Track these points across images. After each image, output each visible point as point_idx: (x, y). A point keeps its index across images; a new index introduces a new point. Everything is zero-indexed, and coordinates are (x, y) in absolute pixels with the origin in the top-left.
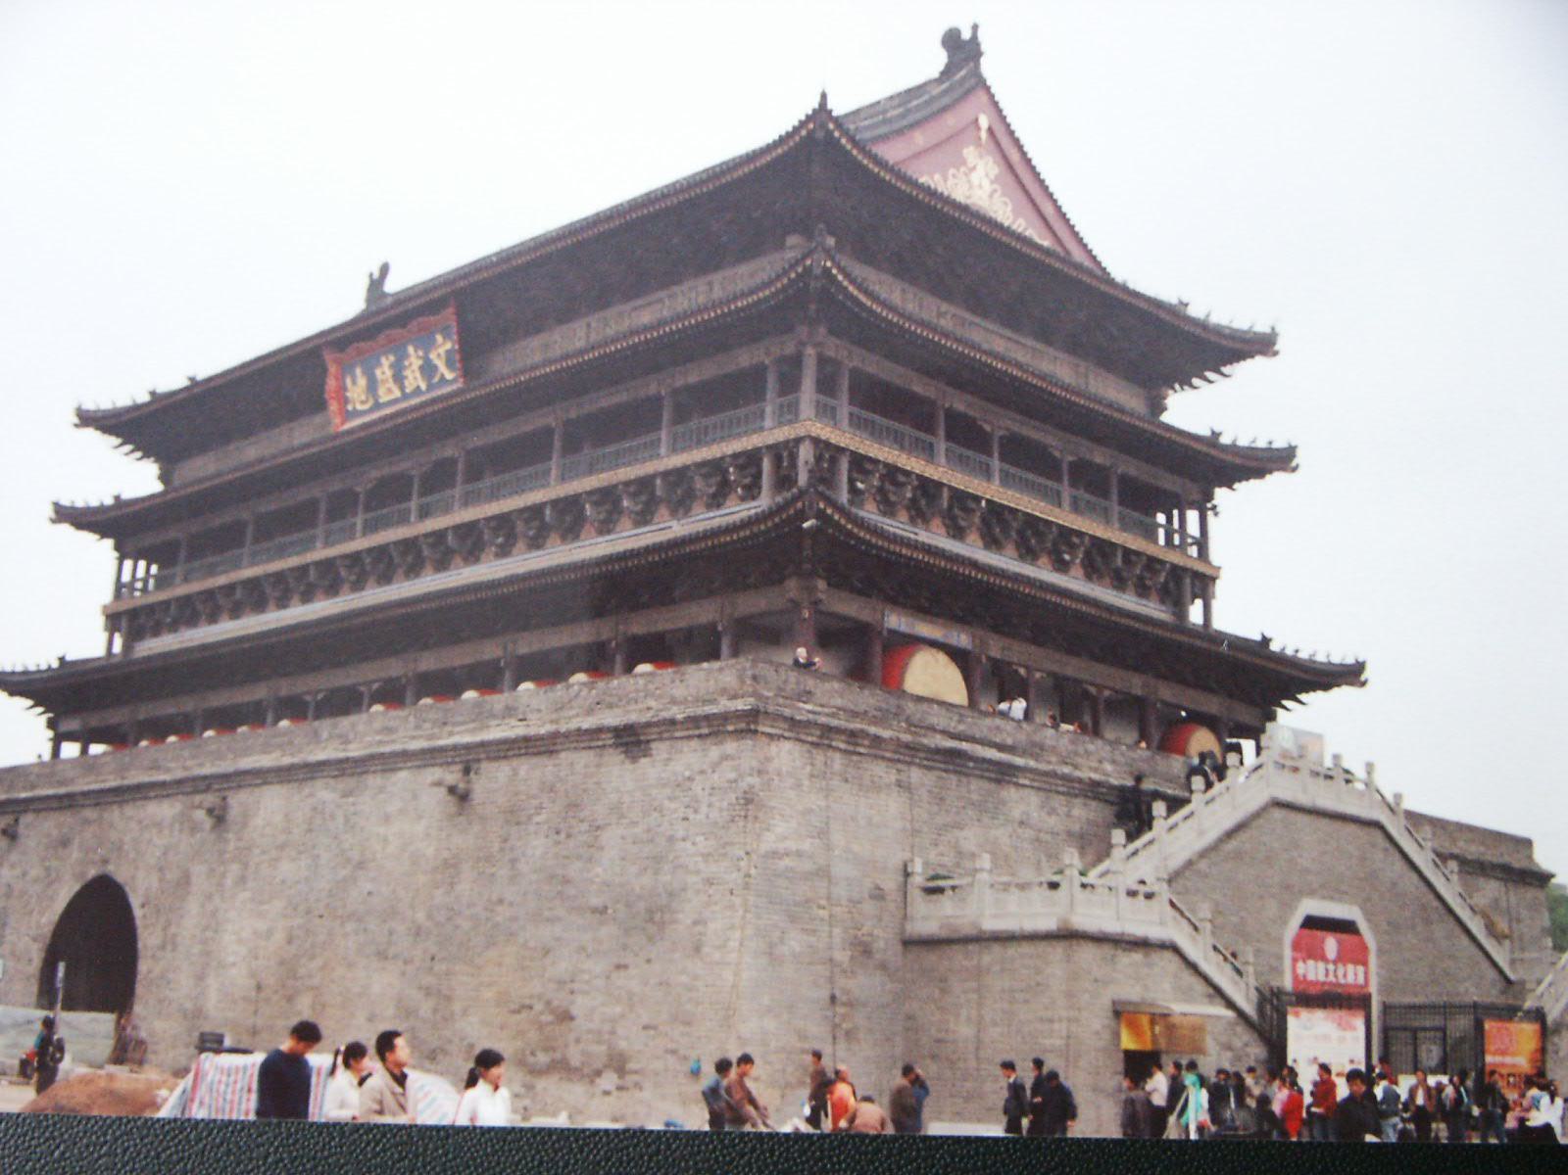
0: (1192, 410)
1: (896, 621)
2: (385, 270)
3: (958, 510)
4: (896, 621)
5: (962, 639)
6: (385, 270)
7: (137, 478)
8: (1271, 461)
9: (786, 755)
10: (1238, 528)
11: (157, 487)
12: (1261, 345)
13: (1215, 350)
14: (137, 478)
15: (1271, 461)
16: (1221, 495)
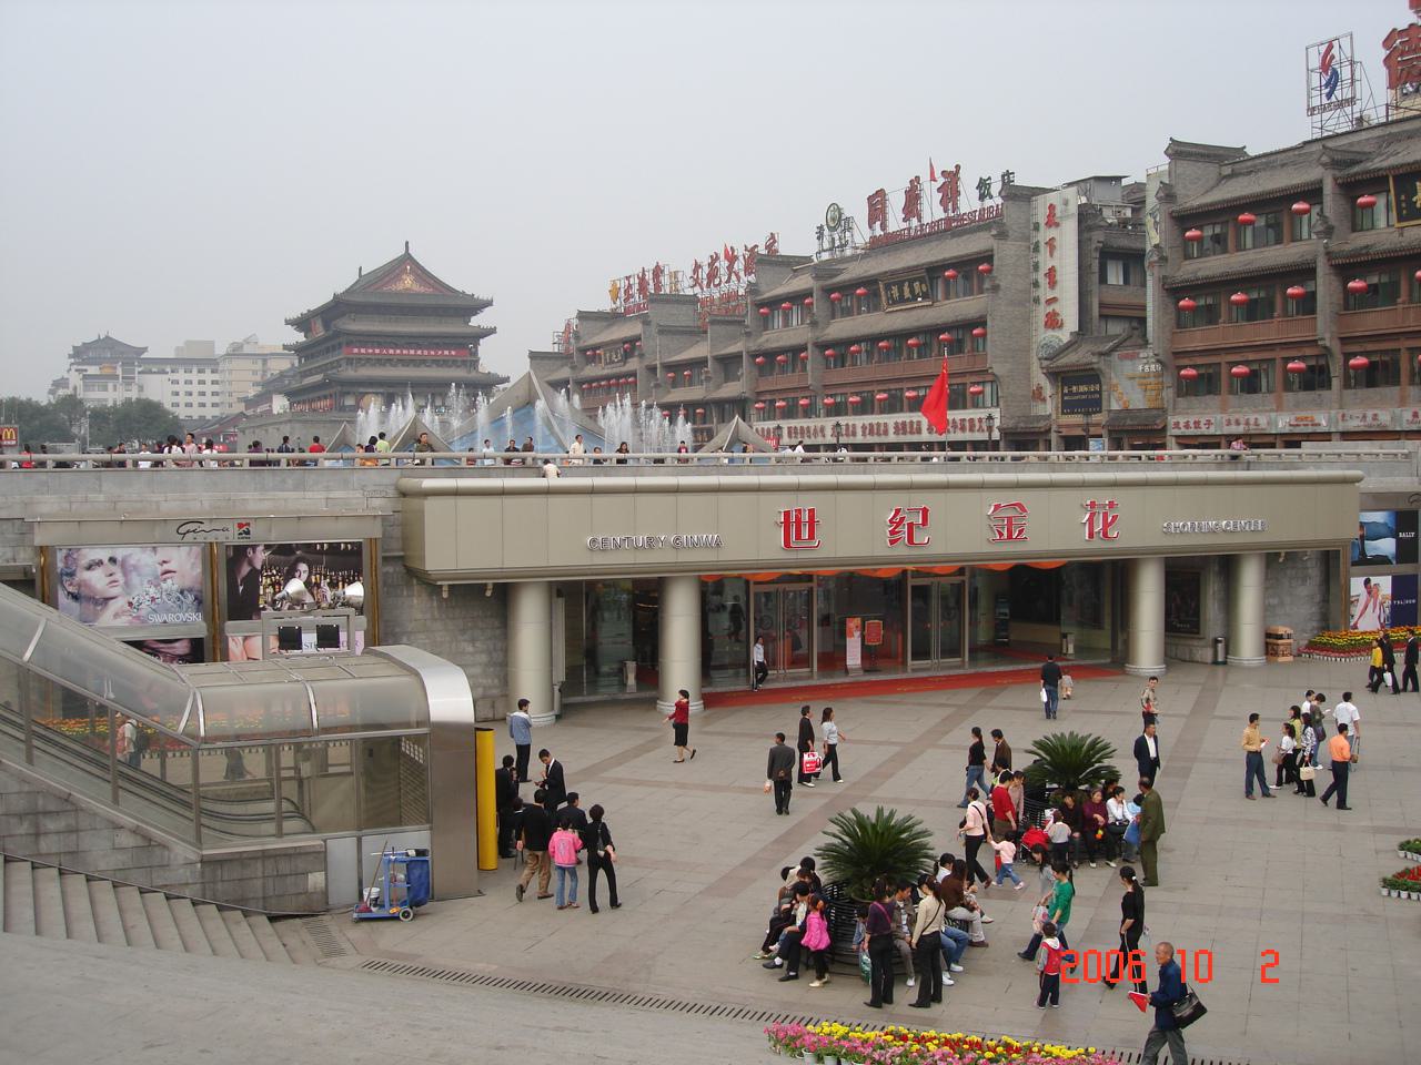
0: (476, 321)
1: (362, 390)
2: (360, 269)
3: (389, 361)
4: (362, 390)
5: (381, 390)
6: (360, 269)
7: (300, 337)
8: (492, 331)
9: (297, 426)
10: (485, 346)
11: (304, 339)
12: (489, 303)
13: (479, 306)
14: (300, 337)
15: (492, 331)
16: (481, 341)
